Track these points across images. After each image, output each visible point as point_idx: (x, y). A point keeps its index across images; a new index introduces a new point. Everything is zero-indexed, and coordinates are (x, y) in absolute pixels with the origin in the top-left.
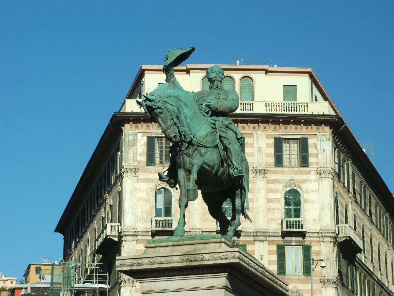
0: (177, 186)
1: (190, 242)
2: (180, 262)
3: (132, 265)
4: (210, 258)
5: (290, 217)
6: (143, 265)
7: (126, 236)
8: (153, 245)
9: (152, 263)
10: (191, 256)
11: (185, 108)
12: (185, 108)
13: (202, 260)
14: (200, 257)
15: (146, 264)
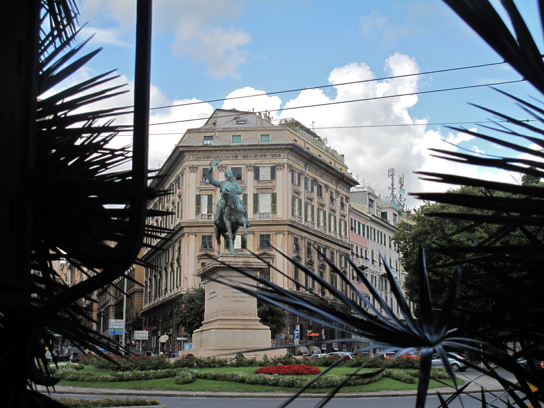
1: (242, 256)
13: (252, 265)
14: (251, 264)
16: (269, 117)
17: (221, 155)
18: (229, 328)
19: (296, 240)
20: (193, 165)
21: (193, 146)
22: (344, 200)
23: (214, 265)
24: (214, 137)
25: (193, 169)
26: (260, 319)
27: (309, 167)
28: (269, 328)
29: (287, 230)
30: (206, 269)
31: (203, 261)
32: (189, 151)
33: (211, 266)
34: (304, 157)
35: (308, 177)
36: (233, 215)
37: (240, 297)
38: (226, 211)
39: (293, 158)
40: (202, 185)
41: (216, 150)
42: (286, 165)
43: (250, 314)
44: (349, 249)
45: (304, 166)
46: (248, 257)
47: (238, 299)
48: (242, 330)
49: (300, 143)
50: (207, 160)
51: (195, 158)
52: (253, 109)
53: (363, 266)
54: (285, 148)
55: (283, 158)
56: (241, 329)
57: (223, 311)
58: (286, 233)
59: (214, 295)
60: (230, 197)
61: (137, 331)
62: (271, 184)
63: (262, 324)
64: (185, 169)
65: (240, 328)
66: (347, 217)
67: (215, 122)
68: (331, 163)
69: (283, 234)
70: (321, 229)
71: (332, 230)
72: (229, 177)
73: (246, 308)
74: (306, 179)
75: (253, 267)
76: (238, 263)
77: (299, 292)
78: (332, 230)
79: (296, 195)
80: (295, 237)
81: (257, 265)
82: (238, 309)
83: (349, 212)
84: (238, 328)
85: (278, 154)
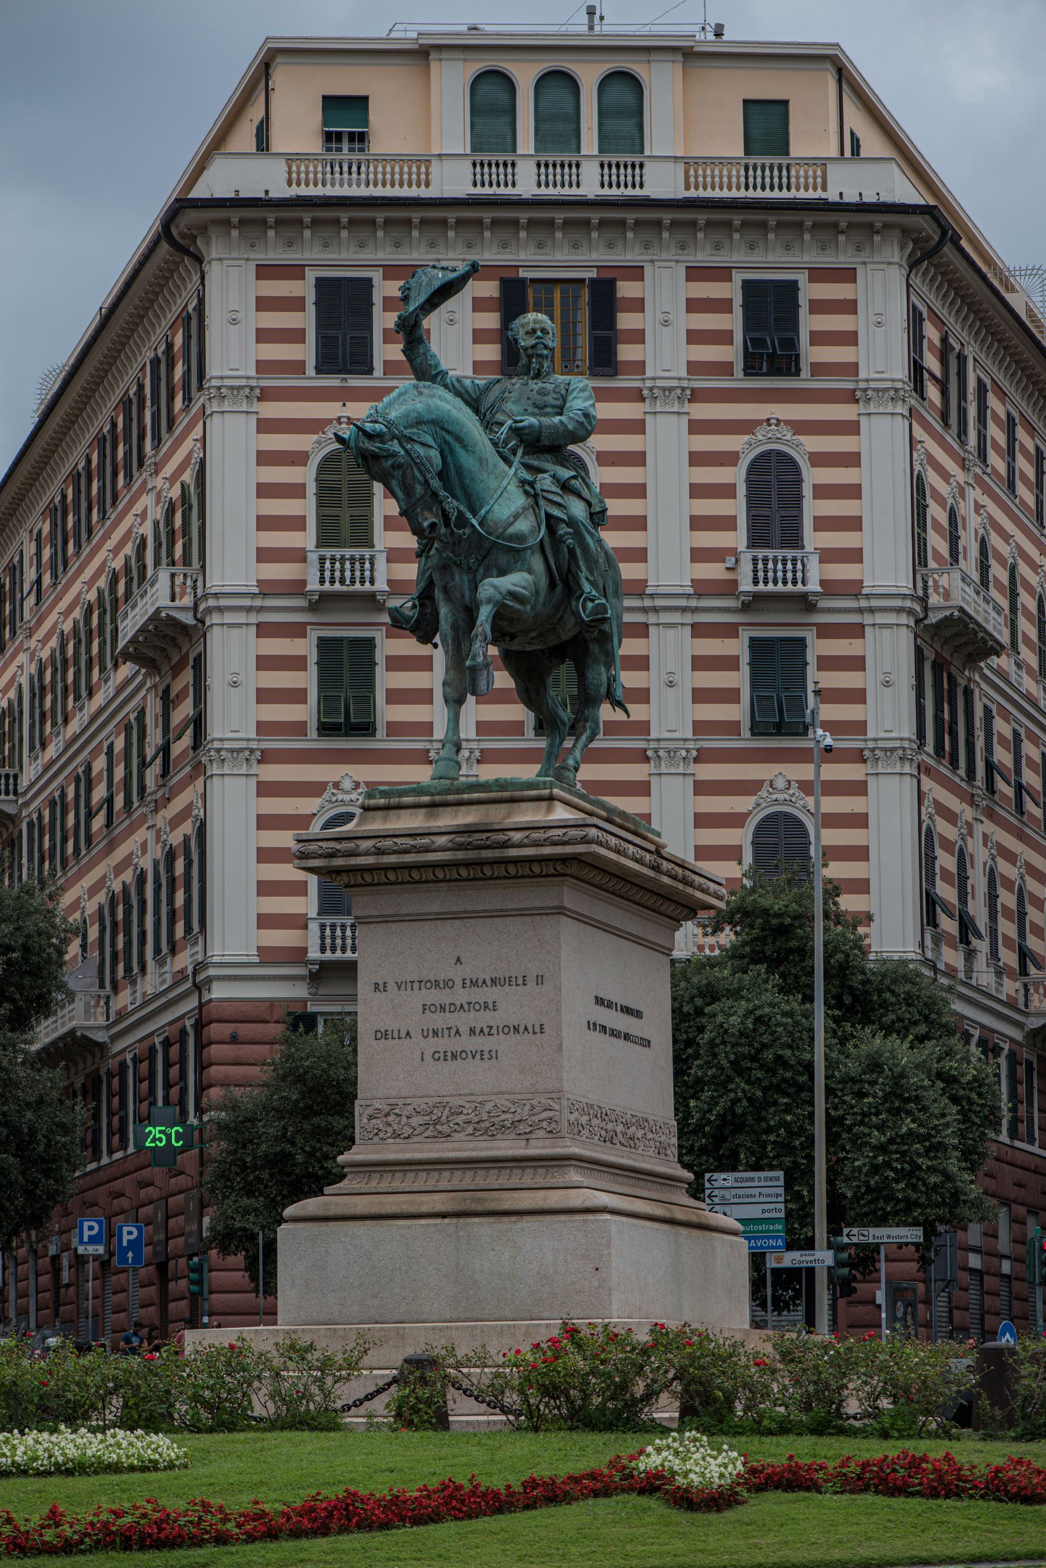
0: (437, 639)
1: (475, 796)
3: (332, 855)
4: (526, 841)
5: (768, 545)
6: (359, 855)
7: (220, 609)
8: (382, 801)
9: (380, 852)
10: (478, 836)
11: (457, 447)
12: (457, 447)
13: (506, 845)
14: (501, 837)
15: (367, 853)
18: (374, 1210)
37: (464, 1030)
43: (523, 1128)
46: (512, 800)
48: (446, 1221)
56: (444, 1216)
57: (371, 1118)
65: (440, 1207)
72: (525, 349)
73: (497, 1093)
75: (513, 852)
76: (425, 841)
81: (536, 844)
84: (424, 1209)
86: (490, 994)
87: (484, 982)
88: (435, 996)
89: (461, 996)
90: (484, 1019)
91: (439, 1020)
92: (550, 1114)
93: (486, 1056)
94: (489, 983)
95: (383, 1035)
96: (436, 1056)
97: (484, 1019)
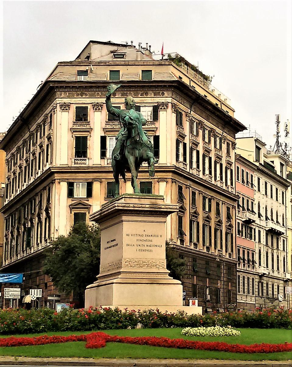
2: (149, 208)
3: (124, 207)
4: (165, 208)
8: (128, 196)
9: (134, 207)
10: (155, 206)
14: (159, 206)
16: (150, 51)
17: (96, 93)
19: (180, 188)
20: (65, 103)
21: (65, 81)
22: (230, 146)
23: (116, 208)
24: (89, 71)
25: (65, 107)
26: (169, 272)
27: (195, 108)
28: (180, 282)
29: (171, 177)
30: (104, 212)
31: (77, 211)
32: (61, 87)
33: (111, 209)
34: (190, 97)
35: (193, 119)
36: (137, 149)
38: (128, 144)
39: (178, 97)
40: (75, 126)
41: (91, 87)
42: (170, 104)
43: (157, 266)
44: (235, 200)
45: (189, 107)
47: (144, 248)
48: (149, 284)
49: (186, 80)
50: (81, 97)
51: (67, 95)
52: (132, 42)
53: (250, 219)
54: (170, 86)
55: (166, 97)
58: (170, 180)
59: (114, 243)
60: (134, 127)
61: (7, 289)
62: (153, 126)
63: (172, 278)
64: (56, 107)
66: (233, 165)
67: (89, 55)
68: (217, 104)
69: (166, 182)
70: (206, 178)
71: (218, 179)
74: (191, 122)
77: (183, 246)
78: (218, 179)
79: (180, 139)
80: (179, 185)
81: (166, 209)
82: (144, 260)
83: (235, 160)
85: (161, 92)
86: (150, 238)
87: (150, 236)
88: (139, 238)
89: (145, 238)
90: (149, 243)
91: (140, 243)
92: (163, 264)
93: (150, 251)
94: (151, 236)
95: (128, 245)
96: (140, 250)
97: (149, 243)
